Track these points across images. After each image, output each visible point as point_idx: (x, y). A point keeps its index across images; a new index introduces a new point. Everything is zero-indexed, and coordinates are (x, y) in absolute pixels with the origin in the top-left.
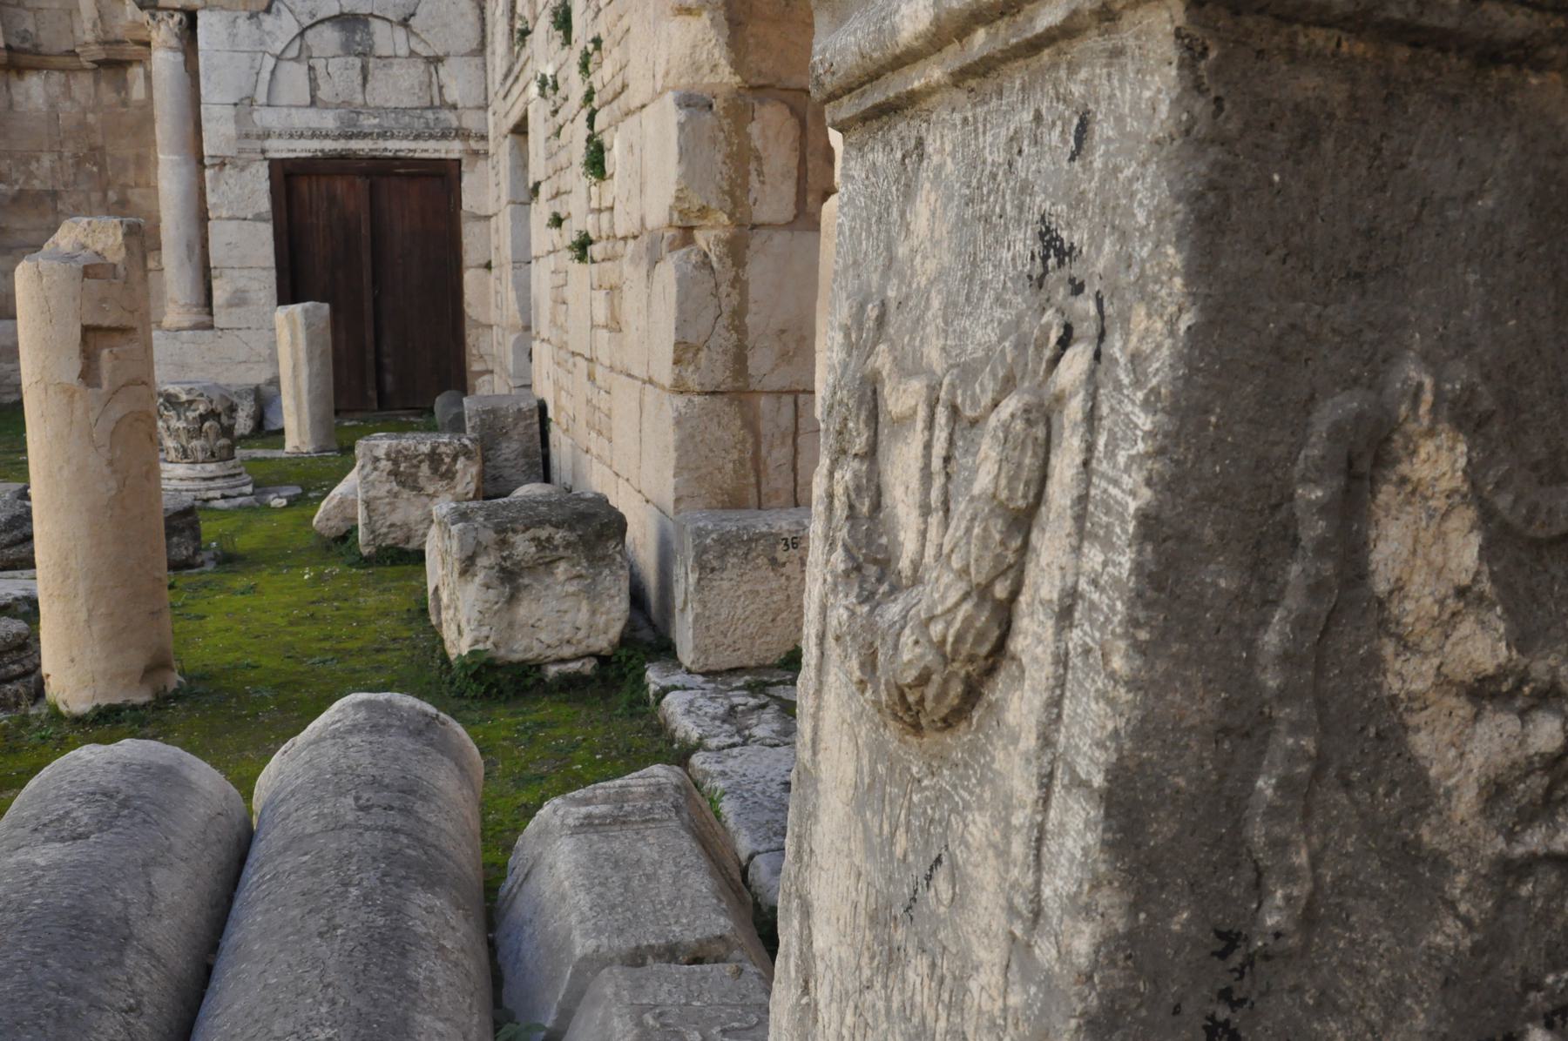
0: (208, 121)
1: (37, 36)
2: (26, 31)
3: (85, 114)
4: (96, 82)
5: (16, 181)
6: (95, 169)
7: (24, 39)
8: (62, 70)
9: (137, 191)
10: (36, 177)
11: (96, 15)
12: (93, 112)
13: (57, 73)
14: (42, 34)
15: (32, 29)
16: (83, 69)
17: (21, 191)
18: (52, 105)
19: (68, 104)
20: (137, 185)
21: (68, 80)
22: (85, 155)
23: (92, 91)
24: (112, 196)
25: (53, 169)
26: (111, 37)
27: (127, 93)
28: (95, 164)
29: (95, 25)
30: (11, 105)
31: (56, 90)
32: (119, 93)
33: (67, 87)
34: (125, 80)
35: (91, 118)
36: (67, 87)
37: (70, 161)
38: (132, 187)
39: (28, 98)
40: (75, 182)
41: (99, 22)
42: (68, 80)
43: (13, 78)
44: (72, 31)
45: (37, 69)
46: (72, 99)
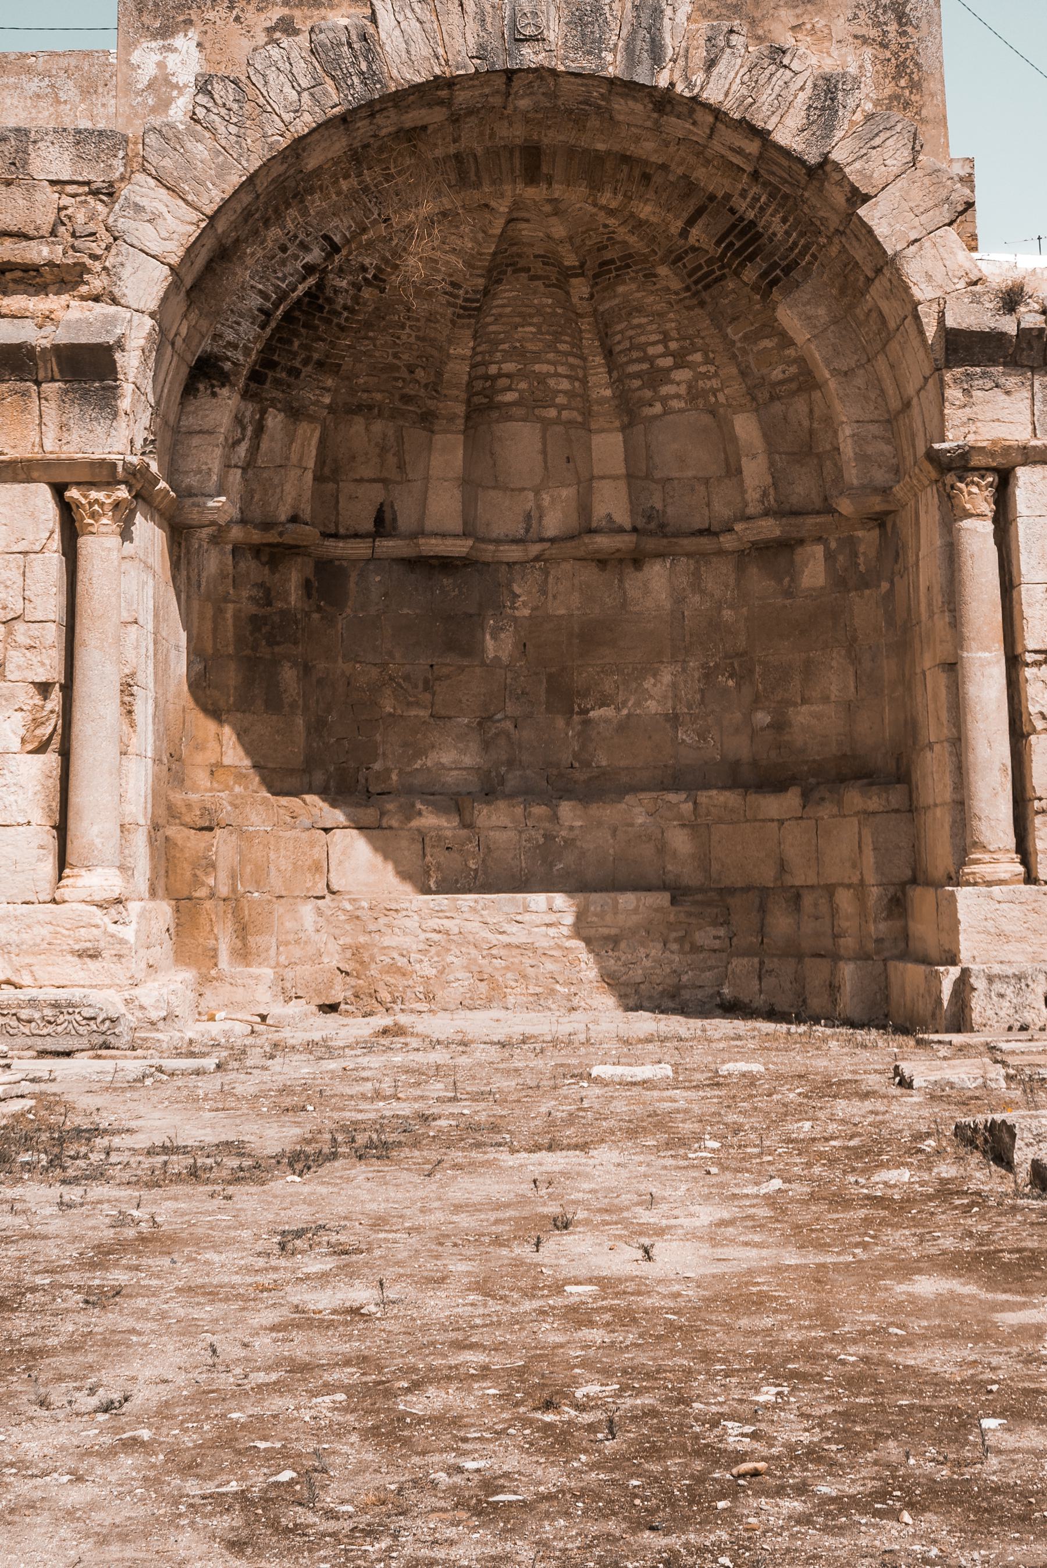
0: (1030, 605)
1: (664, 512)
2: (652, 508)
3: (719, 609)
4: (740, 568)
5: (624, 703)
6: (731, 683)
7: (650, 519)
8: (689, 555)
9: (804, 709)
10: (651, 697)
11: (769, 480)
12: (731, 607)
13: (684, 559)
14: (670, 510)
15: (659, 506)
16: (721, 552)
17: (629, 716)
18: (679, 600)
19: (697, 598)
20: (804, 701)
21: (697, 569)
22: (717, 665)
23: (732, 581)
24: (762, 718)
25: (674, 685)
26: (787, 507)
27: (792, 580)
28: (731, 676)
29: (765, 494)
30: (624, 605)
31: (684, 581)
32: (780, 581)
33: (697, 574)
34: (792, 562)
35: (727, 614)
36: (697, 574)
37: (696, 675)
38: (795, 704)
39: (646, 591)
40: (702, 701)
41: (772, 491)
42: (697, 569)
43: (629, 570)
44: (708, 505)
45: (661, 555)
46: (702, 592)
